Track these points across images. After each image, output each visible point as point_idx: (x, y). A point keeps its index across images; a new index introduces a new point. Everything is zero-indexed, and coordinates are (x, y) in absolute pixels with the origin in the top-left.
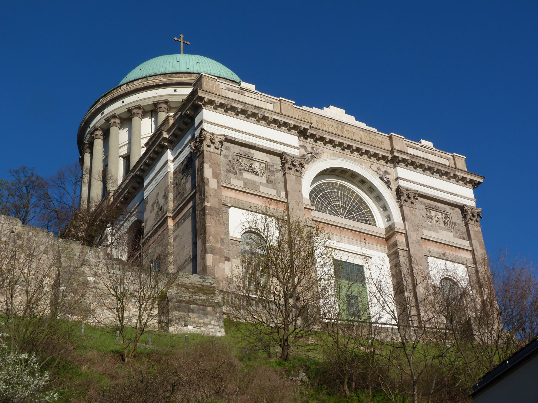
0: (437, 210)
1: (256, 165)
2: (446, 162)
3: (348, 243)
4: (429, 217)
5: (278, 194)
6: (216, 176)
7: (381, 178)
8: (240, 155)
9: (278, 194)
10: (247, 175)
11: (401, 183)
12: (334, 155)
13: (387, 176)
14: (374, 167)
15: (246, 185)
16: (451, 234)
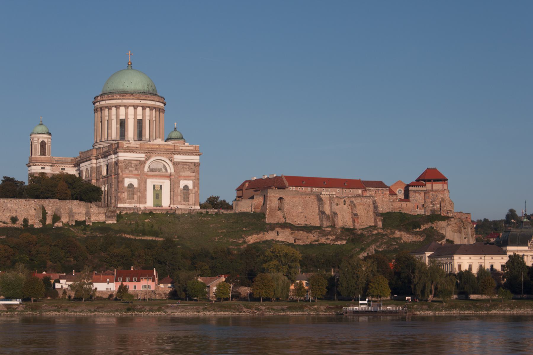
0: (186, 165)
1: (133, 165)
2: (192, 148)
3: (158, 179)
4: (183, 168)
5: (138, 172)
6: (122, 172)
7: (169, 160)
8: (128, 163)
9: (138, 172)
10: (130, 169)
11: (175, 160)
12: (156, 156)
13: (172, 158)
14: (168, 157)
15: (129, 171)
16: (189, 172)
